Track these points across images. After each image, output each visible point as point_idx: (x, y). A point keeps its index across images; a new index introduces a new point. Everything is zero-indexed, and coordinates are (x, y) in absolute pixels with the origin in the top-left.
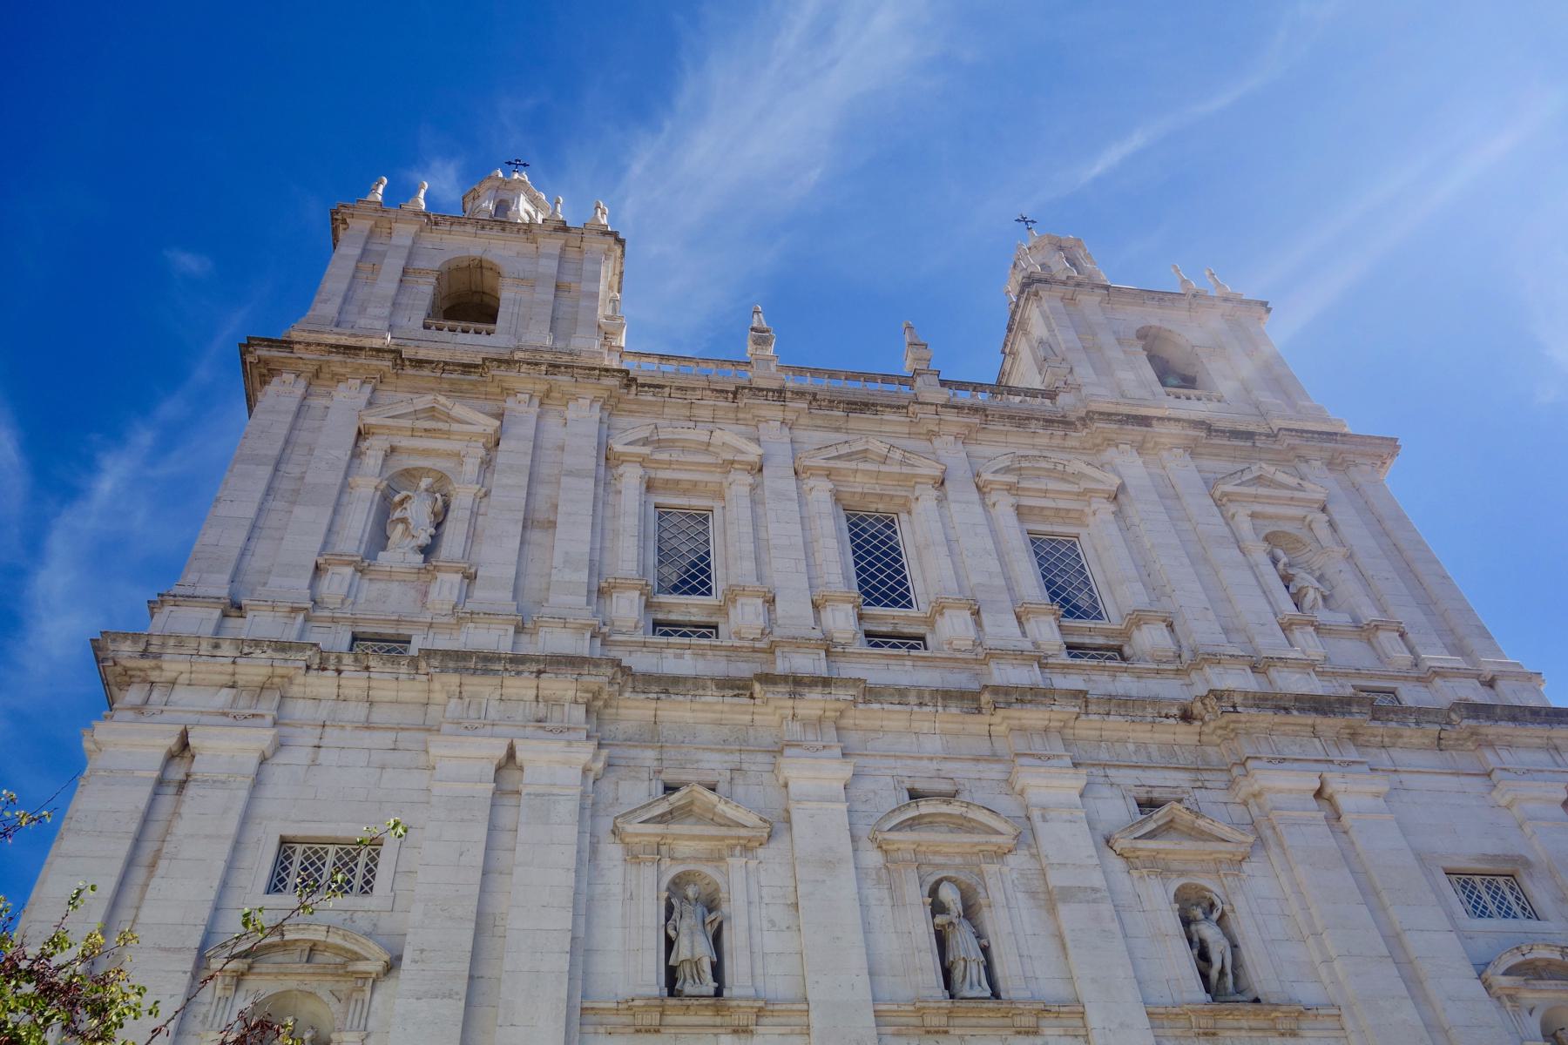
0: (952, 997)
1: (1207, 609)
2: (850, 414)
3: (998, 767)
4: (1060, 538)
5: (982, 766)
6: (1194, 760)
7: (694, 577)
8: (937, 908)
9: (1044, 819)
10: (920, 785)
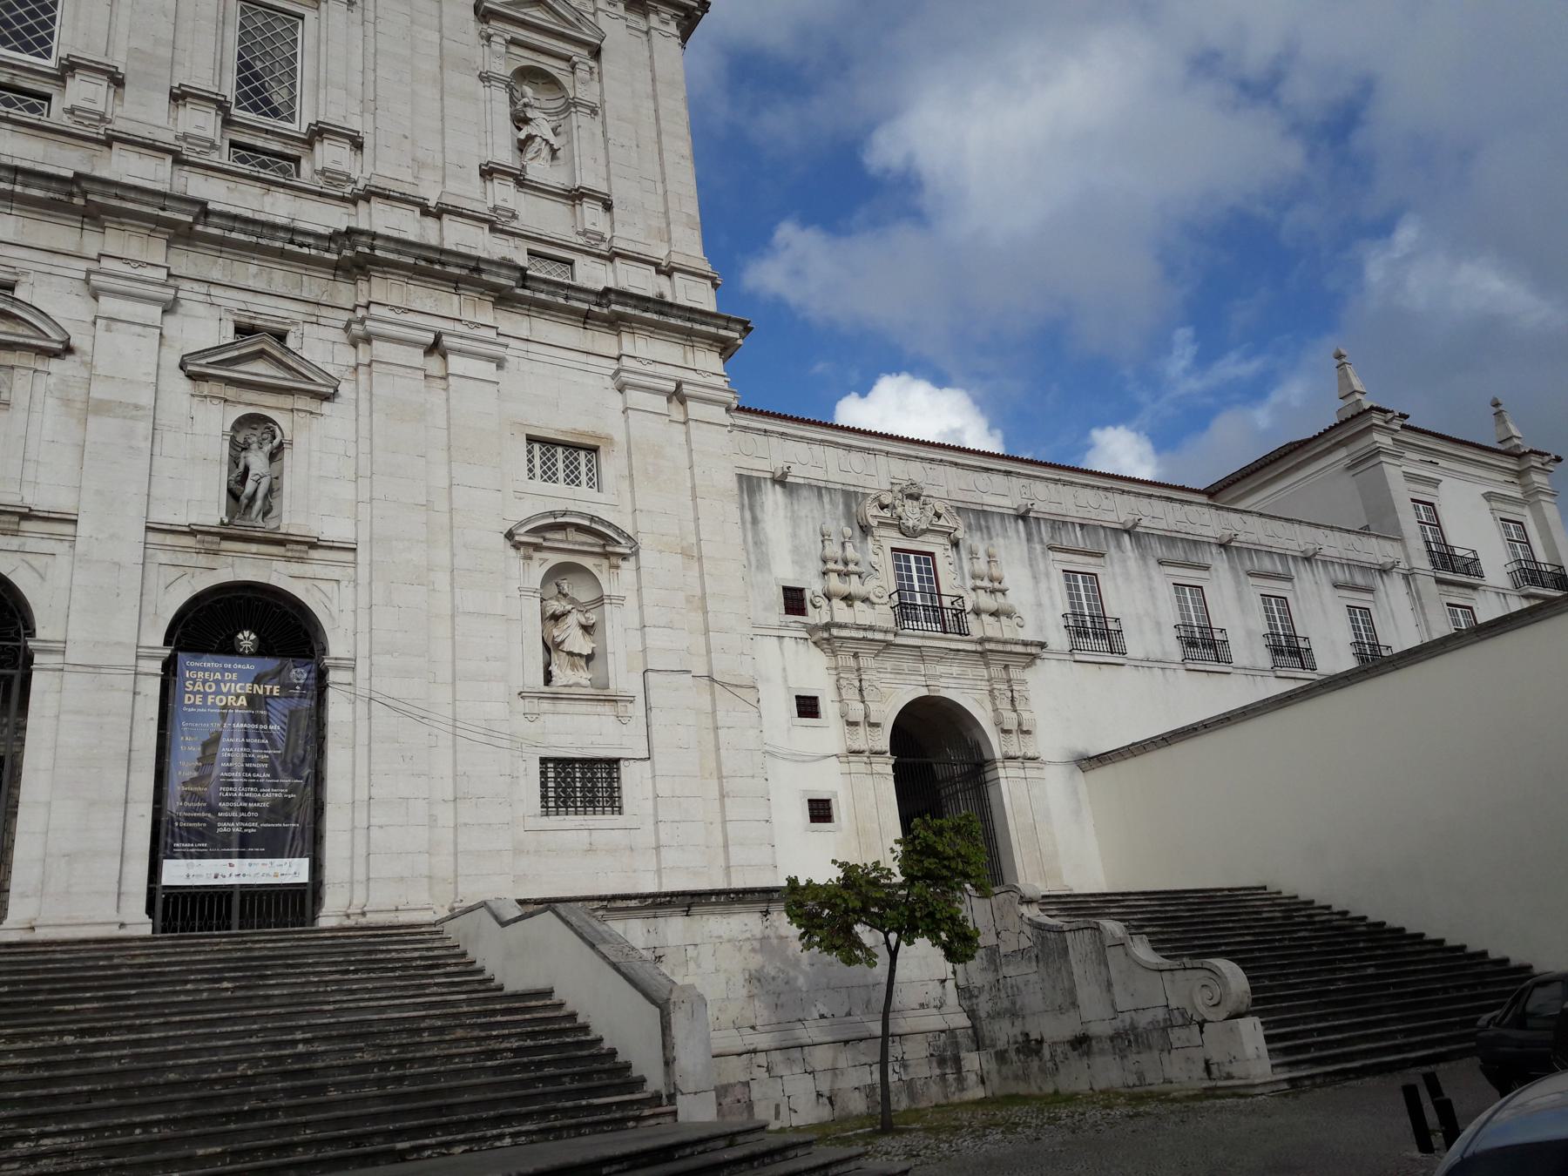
1: (406, 138)
3: (84, 265)
4: (280, 15)
5: (58, 260)
6: (320, 294)
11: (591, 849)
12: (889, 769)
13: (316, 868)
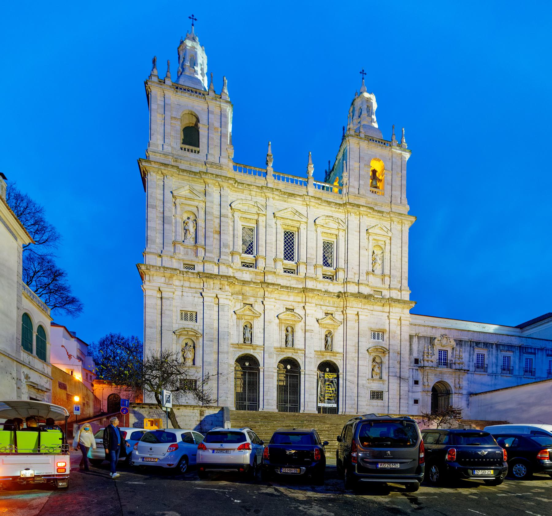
0: (286, 346)
2: (289, 197)
7: (250, 249)
8: (287, 331)
10: (288, 307)
11: (377, 406)
12: (431, 395)
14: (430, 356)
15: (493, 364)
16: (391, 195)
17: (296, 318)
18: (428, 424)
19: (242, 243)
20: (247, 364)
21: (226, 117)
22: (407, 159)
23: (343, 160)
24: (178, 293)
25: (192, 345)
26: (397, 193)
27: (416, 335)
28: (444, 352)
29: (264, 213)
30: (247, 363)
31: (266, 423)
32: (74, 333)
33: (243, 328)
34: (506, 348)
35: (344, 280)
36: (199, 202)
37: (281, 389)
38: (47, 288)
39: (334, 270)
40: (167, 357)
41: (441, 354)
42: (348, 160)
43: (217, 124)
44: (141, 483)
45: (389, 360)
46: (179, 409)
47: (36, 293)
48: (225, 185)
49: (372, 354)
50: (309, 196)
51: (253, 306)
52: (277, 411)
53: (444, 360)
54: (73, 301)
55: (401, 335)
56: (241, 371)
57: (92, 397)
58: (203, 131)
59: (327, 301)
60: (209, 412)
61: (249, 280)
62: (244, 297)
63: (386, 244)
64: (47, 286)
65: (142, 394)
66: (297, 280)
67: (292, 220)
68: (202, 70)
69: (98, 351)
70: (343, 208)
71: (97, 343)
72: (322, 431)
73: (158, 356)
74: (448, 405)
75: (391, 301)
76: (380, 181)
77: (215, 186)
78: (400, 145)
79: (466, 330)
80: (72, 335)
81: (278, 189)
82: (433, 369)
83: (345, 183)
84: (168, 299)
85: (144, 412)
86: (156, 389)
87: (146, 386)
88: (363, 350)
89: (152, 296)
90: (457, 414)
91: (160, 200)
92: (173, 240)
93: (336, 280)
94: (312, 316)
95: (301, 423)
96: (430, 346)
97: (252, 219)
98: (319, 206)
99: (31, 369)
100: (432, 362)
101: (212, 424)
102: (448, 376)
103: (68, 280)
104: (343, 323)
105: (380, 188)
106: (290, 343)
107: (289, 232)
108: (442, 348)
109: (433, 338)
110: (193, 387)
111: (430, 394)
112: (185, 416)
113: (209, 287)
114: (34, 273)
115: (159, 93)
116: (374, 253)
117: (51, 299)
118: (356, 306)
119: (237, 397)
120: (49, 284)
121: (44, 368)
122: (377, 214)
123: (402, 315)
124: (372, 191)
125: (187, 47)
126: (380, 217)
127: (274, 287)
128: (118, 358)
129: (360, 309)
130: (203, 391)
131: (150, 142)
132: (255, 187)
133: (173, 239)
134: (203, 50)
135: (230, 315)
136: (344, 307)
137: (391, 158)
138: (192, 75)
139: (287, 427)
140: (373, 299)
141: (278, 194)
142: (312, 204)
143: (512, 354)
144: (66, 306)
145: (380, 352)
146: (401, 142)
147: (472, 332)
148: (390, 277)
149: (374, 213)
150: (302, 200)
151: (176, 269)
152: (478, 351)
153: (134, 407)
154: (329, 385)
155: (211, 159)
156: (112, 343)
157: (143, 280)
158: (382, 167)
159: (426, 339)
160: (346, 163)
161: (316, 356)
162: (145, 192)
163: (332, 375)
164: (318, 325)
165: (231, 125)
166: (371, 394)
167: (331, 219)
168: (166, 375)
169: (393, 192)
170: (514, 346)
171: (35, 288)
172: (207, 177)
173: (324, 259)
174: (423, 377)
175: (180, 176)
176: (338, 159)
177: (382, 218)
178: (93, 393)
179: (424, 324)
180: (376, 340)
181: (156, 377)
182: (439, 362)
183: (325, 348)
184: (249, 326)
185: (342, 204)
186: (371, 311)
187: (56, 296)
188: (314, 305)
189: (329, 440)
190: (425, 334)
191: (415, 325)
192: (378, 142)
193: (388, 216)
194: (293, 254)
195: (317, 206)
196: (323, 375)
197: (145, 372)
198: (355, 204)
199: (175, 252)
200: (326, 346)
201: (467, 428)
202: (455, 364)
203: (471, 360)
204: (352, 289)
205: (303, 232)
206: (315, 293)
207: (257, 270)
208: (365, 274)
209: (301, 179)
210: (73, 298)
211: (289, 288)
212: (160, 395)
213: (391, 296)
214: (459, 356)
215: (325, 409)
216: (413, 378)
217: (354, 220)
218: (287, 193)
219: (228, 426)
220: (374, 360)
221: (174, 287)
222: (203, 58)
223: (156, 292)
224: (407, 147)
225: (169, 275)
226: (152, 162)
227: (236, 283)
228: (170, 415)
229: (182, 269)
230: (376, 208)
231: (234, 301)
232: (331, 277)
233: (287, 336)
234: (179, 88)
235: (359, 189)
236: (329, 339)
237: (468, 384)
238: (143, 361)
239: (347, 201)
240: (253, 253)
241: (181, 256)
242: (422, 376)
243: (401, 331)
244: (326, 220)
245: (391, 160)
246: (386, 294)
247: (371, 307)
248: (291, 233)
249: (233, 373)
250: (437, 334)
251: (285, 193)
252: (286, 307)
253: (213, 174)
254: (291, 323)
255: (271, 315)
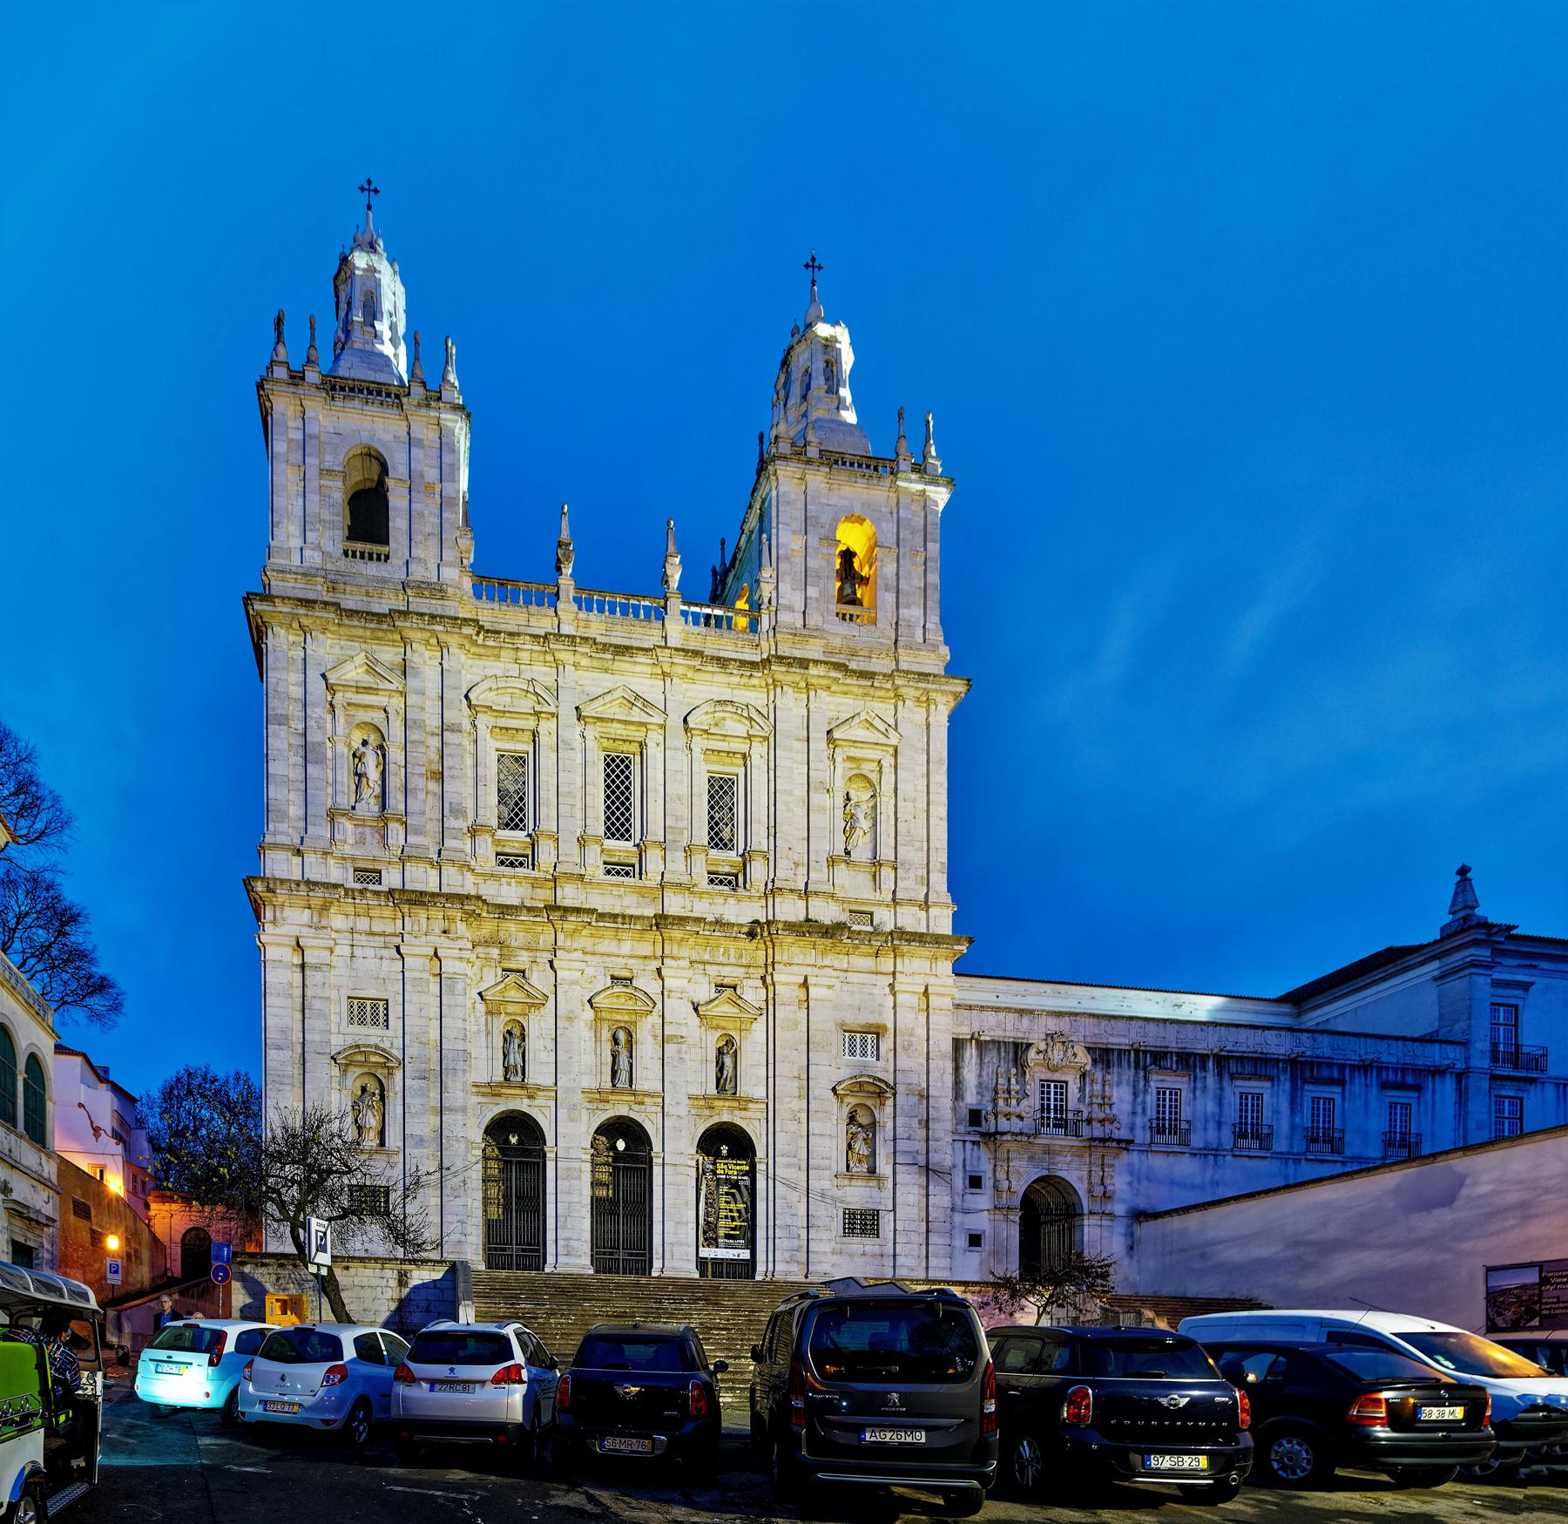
0: (614, 1086)
8: (616, 1041)
9: (669, 997)
10: (616, 974)
11: (864, 1254)
13: (753, 1254)
14: (1014, 1102)
15: (1206, 1120)
16: (895, 621)
17: (639, 1003)
18: (1009, 1309)
19: (497, 799)
20: (514, 1140)
21: (454, 451)
22: (941, 508)
23: (761, 532)
24: (343, 951)
25: (377, 1092)
26: (913, 613)
27: (972, 1038)
28: (1056, 1087)
29: (552, 709)
30: (513, 1137)
31: (565, 1307)
32: (106, 1070)
33: (502, 1039)
34: (1249, 1068)
35: (766, 884)
36: (390, 696)
37: (601, 1209)
38: (46, 956)
39: (740, 859)
40: (318, 1127)
41: (1049, 1093)
42: (774, 531)
43: (432, 474)
44: (261, 1471)
45: (895, 1117)
46: (347, 1268)
47: (23, 970)
48: (453, 640)
49: (847, 1100)
50: (669, 648)
51: (527, 974)
52: (591, 1272)
53: (1056, 1113)
54: (101, 986)
55: (928, 1040)
56: (500, 1160)
57: (146, 1237)
58: (397, 500)
59: (722, 950)
60: (420, 1276)
61: (516, 902)
62: (505, 951)
63: (883, 769)
64: (45, 952)
65: (259, 1225)
66: (641, 892)
67: (626, 722)
68: (393, 327)
69: (158, 1116)
70: (760, 674)
71: (156, 1093)
72: (712, 1329)
73: (297, 1123)
74: (1071, 1250)
75: (900, 940)
76: (864, 581)
77: (429, 647)
78: (919, 468)
79: (1123, 1017)
80: (101, 1075)
81: (585, 639)
82: (1024, 1139)
83: (766, 600)
84: (317, 968)
85: (264, 1276)
86: (292, 1214)
87: (271, 1208)
88: (821, 1089)
89: (281, 961)
90: (1098, 1276)
91: (296, 700)
92: (329, 806)
93: (745, 888)
94: (679, 995)
95: (654, 1306)
96: (1014, 1071)
97: (523, 730)
98: (697, 676)
99: (13, 1167)
100: (1020, 1117)
101: (428, 1310)
102: (1068, 1158)
103: (90, 933)
104: (765, 1011)
105: (865, 603)
106: (624, 1076)
107: (618, 757)
108: (1049, 1076)
109: (1024, 1047)
110: (380, 1206)
111: (1016, 1217)
112: (363, 1287)
113: (416, 928)
114: (18, 919)
115: (292, 407)
116: (848, 799)
117: (54, 985)
118: (798, 959)
119: (489, 1234)
120: (50, 945)
121: (41, 1164)
122: (855, 682)
123: (931, 980)
124: (841, 615)
125: (357, 272)
126: (865, 691)
127: (579, 920)
128: (204, 1132)
129: (810, 969)
130: (405, 1217)
131: (273, 544)
132: (528, 638)
133: (330, 803)
134: (395, 272)
135: (469, 1003)
136: (766, 965)
137: (895, 510)
138: (368, 348)
139: (616, 1317)
140: (848, 938)
141: (587, 650)
142: (679, 670)
143: (1268, 1084)
144: (87, 999)
145: (868, 1092)
146: (924, 457)
147: (1141, 1023)
148: (896, 869)
149: (849, 681)
150: (652, 662)
151: (336, 886)
152: (1157, 1080)
153: (243, 1263)
154: (727, 1194)
155: (418, 573)
156: (190, 1093)
157: (259, 919)
158: (869, 539)
159: (1002, 1050)
160: (769, 539)
161: (693, 1112)
162: (262, 681)
163: (736, 1165)
164: (697, 1020)
165: (467, 471)
166: (845, 1219)
167: (729, 708)
168: (315, 1176)
169: (901, 611)
170: (1274, 1059)
171: (19, 958)
172: (408, 624)
173: (712, 828)
174: (995, 1166)
175: (343, 630)
176: (746, 531)
177: (872, 691)
178: (148, 1226)
179: (997, 1005)
180: (858, 1057)
181: (293, 1181)
182: (1043, 1118)
183: (717, 1088)
184: (517, 1031)
185: (758, 663)
186: (841, 974)
187: (65, 976)
188: (685, 963)
189: (731, 1357)
190: (998, 1034)
191: (970, 1008)
192: (856, 465)
193: (889, 686)
194: (627, 820)
195: (690, 674)
196: (711, 1167)
197: (267, 1170)
198: (794, 658)
199: (333, 837)
200: (718, 1080)
201: (1126, 1321)
202: (1089, 1121)
203: (1139, 1109)
204: (790, 909)
205: (654, 752)
206: (688, 928)
207: (535, 874)
208: (825, 864)
209: (647, 603)
210: (103, 979)
211: (620, 920)
212: (301, 1231)
213: (899, 925)
214: (1103, 1098)
215: (717, 1263)
216: (965, 1171)
217: (791, 705)
218: (611, 645)
219: (468, 1317)
220: (852, 1119)
221: (334, 935)
222: (394, 294)
223: (290, 950)
224: (940, 470)
225: (319, 902)
226: (276, 600)
227: (484, 915)
228: (328, 1286)
229: (351, 884)
230: (853, 666)
231: (478, 963)
232: (730, 878)
233: (615, 1057)
234: (337, 387)
235: (804, 612)
236: (728, 1061)
237: (1130, 1184)
238: (261, 1137)
239: (773, 652)
240: (524, 826)
241: (348, 850)
242: (992, 1161)
243: (928, 1030)
244: (717, 715)
245: (895, 516)
246: (885, 918)
247: (841, 961)
248: (622, 761)
249: (480, 1166)
250: (1035, 1032)
251: (605, 647)
252: (611, 973)
253: (422, 615)
254: (626, 1018)
255: (573, 999)
